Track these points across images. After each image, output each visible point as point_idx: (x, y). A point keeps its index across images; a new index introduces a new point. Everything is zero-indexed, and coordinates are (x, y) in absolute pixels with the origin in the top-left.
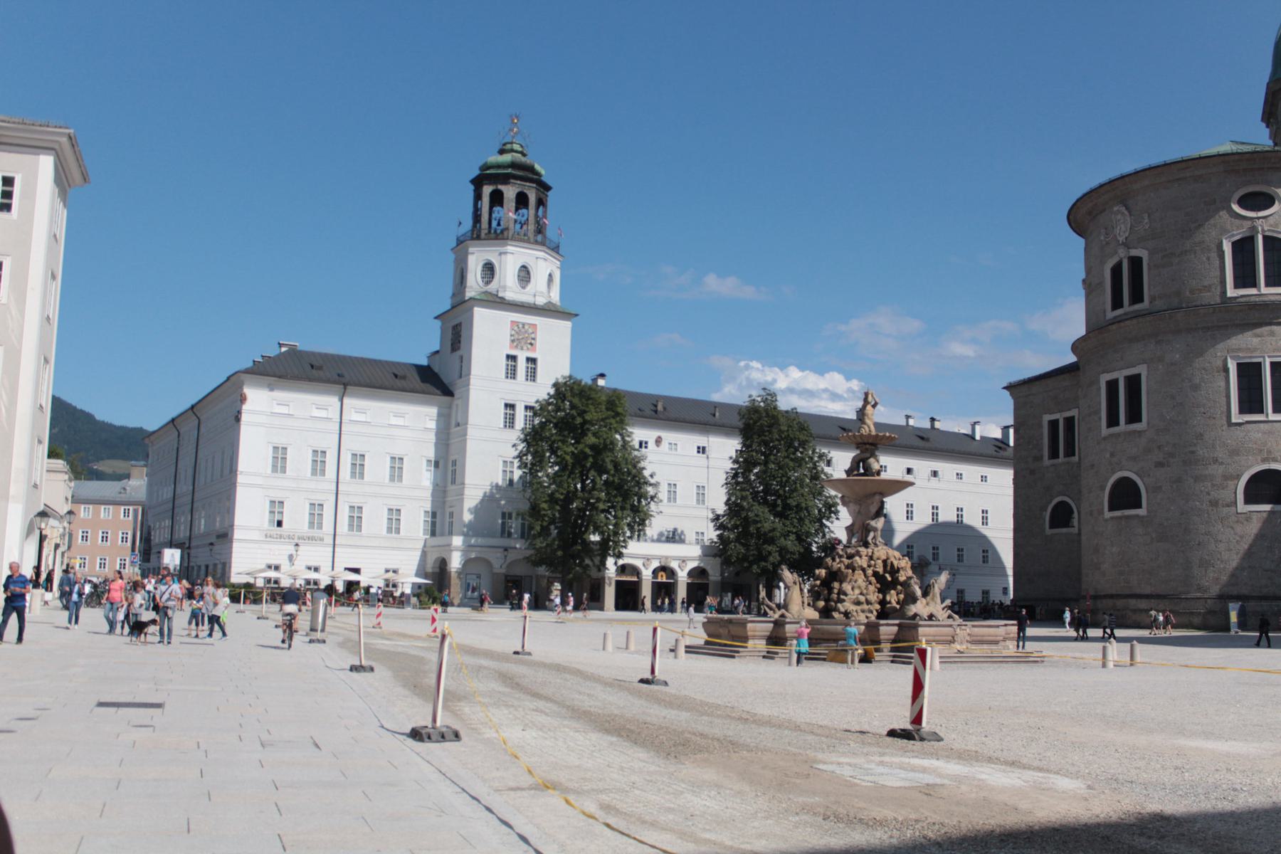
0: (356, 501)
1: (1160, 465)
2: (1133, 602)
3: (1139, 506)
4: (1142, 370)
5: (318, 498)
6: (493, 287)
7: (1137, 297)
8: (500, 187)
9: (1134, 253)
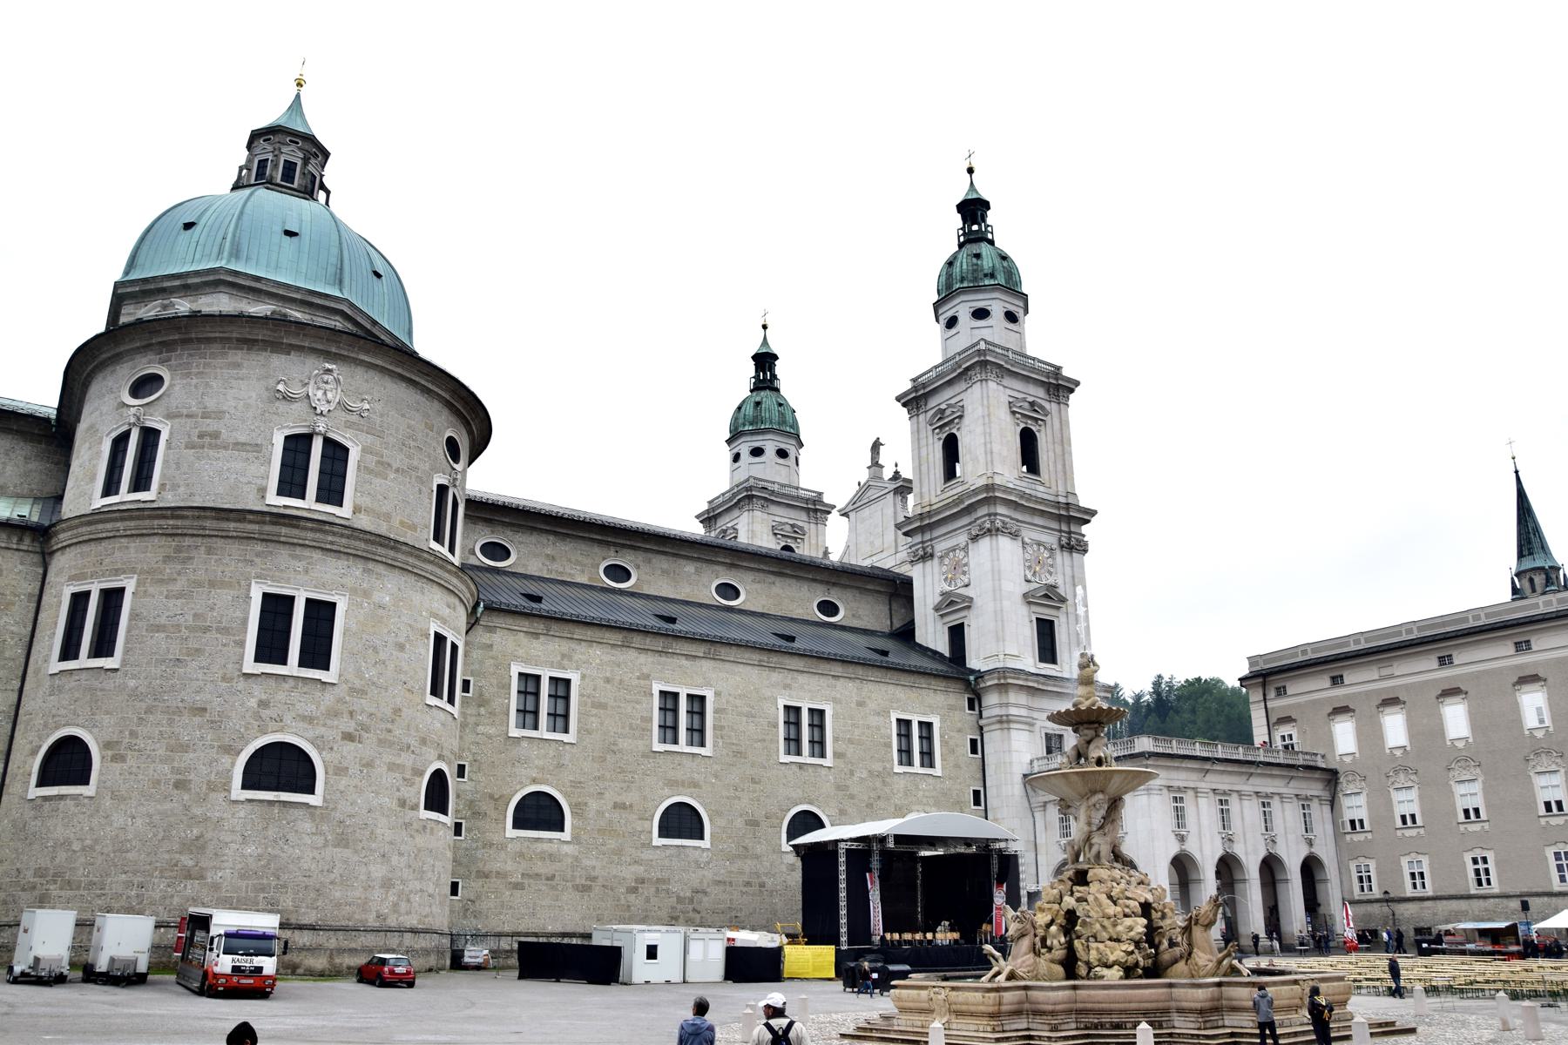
1: (348, 737)
3: (310, 790)
7: (332, 491)
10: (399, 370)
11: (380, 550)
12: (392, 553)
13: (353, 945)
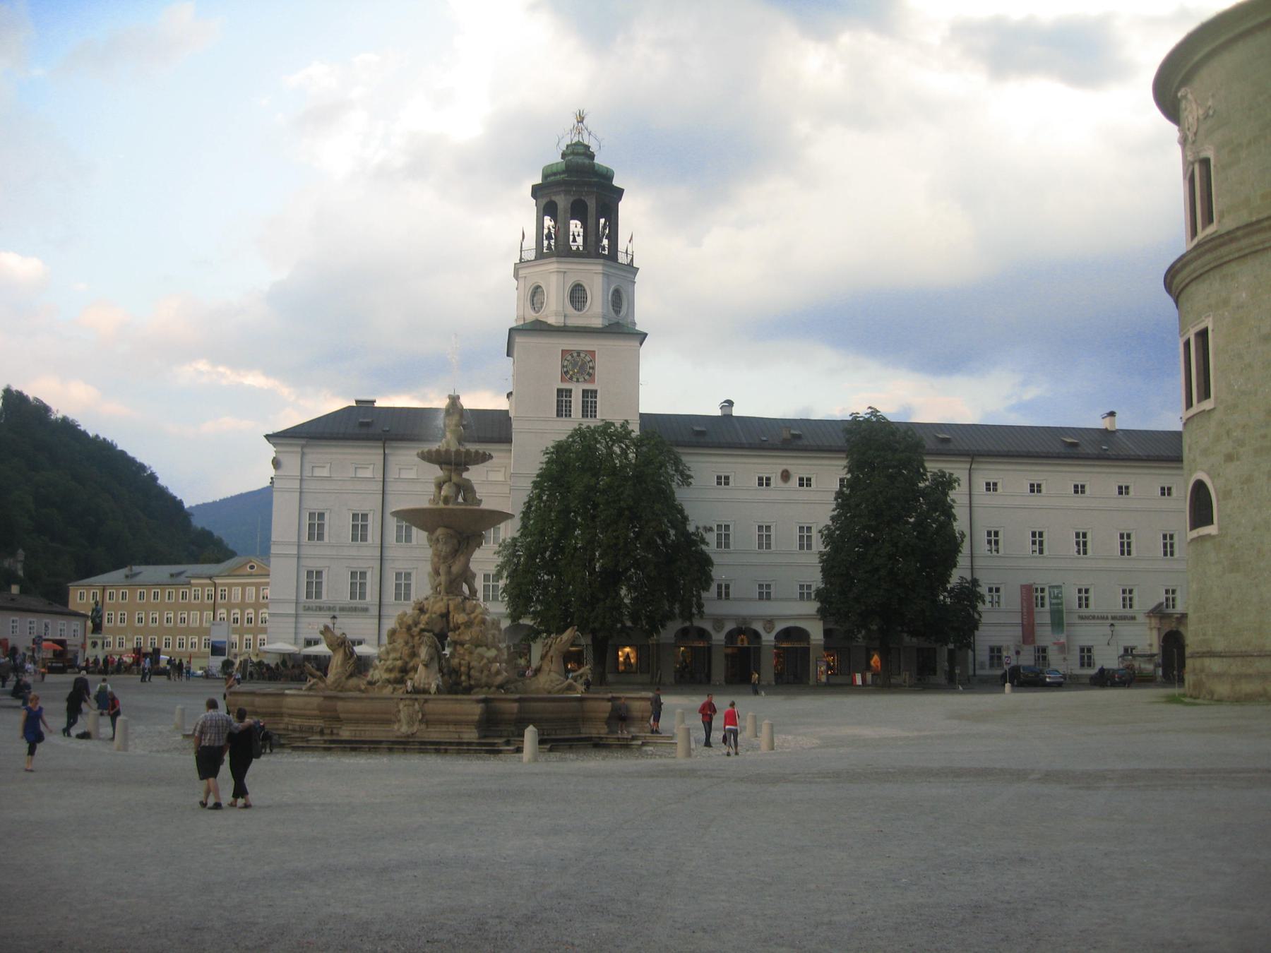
0: (402, 566)
1: (1229, 458)
2: (1207, 661)
4: (1209, 323)
5: (359, 565)
6: (541, 316)
8: (554, 198)
9: (1203, 155)
10: (1223, 39)
11: (1224, 250)
12: (1234, 246)
13: (1250, 671)
